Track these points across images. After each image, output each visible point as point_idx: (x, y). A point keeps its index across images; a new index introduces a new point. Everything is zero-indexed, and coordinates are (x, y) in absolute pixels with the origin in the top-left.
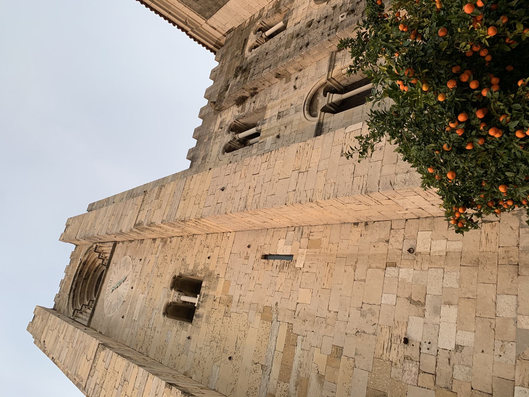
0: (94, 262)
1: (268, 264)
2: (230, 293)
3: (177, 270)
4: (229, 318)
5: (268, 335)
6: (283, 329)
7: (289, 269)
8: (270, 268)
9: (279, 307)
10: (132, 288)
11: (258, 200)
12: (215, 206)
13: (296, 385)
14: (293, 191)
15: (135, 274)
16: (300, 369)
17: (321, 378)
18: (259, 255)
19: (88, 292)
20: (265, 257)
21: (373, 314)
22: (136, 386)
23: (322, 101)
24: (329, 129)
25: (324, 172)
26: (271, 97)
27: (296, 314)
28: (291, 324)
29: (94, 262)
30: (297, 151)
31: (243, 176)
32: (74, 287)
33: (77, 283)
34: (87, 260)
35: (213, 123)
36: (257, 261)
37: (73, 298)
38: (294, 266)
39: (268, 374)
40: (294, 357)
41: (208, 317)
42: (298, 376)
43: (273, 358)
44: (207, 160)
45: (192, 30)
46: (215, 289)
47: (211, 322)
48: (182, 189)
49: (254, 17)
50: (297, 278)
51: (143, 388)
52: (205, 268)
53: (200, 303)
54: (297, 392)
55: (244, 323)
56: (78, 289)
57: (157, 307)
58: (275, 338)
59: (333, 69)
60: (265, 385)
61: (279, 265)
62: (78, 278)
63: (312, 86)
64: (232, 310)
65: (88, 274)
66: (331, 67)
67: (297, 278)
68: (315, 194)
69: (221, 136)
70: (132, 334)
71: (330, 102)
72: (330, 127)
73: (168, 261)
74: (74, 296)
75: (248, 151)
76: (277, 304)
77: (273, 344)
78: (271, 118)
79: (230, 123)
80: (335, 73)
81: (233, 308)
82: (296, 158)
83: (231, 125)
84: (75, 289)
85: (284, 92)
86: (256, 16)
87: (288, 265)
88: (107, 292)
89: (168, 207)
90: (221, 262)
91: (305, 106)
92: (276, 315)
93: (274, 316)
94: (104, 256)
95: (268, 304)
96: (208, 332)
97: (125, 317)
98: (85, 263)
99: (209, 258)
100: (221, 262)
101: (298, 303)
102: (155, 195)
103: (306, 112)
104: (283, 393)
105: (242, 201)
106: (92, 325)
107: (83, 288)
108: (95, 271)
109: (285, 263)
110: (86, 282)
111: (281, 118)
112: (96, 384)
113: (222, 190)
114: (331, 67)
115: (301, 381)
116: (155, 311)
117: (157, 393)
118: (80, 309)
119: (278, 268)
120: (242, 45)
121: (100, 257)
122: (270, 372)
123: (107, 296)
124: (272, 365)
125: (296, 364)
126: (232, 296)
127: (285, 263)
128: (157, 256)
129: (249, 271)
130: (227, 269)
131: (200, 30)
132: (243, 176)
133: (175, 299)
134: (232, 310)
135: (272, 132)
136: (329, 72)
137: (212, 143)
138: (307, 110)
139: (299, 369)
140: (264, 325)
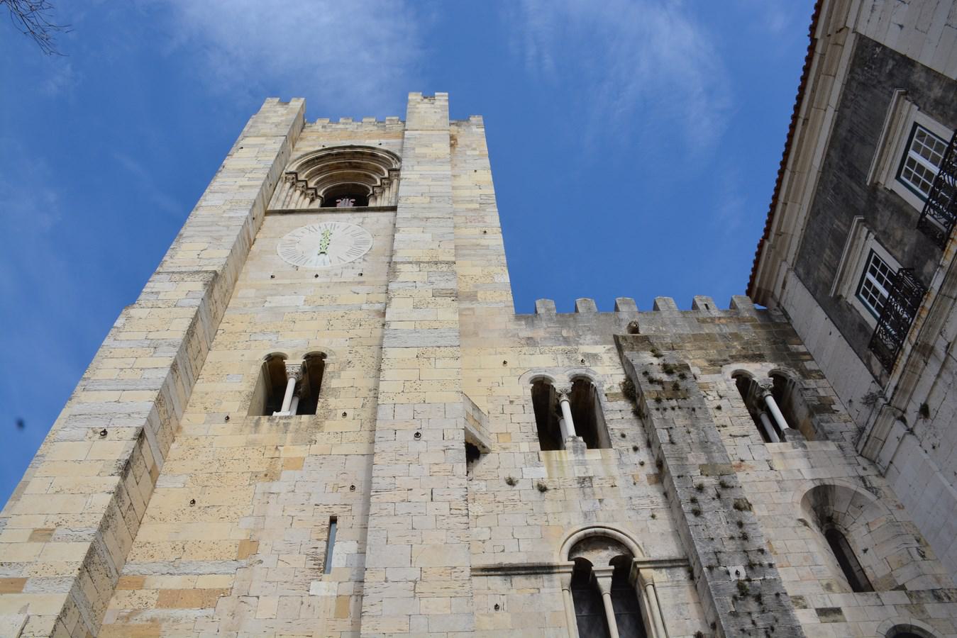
0: (379, 171)
1: (322, 531)
2: (286, 475)
3: (334, 357)
4: (248, 483)
5: (219, 559)
6: (221, 582)
7: (310, 571)
8: (314, 536)
9: (256, 566)
10: (317, 276)
11: (384, 512)
12: (392, 426)
13: (153, 620)
14: (386, 578)
15: (339, 272)
16: (171, 621)
18: (336, 511)
19: (331, 176)
20: (333, 520)
22: (147, 371)
23: (600, 560)
24: (538, 589)
25: (406, 628)
26: (625, 452)
27: (244, 599)
28: (231, 592)
29: (379, 171)
30: (455, 568)
31: (435, 468)
32: (335, 151)
33: (342, 154)
34: (377, 156)
35: (597, 338)
36: (328, 510)
37: (317, 158)
38: (313, 579)
39: (170, 571)
40: (187, 607)
41: (251, 444)
42: (163, 620)
43: (187, 574)
44: (525, 349)
45: (772, 247)
46: (295, 442)
47: (247, 452)
48: (439, 345)
49: (807, 360)
50: (296, 587)
51: (140, 387)
52: (331, 411)
53: (277, 421)
54: (144, 623)
55: (240, 514)
56: (333, 159)
57: (281, 339)
58: (214, 570)
59: (655, 568)
60: (156, 569)
61: (319, 551)
62: (349, 153)
63: (632, 536)
64: (259, 485)
65: (357, 166)
66: (658, 564)
67: (296, 587)
68: (372, 619)
69: (569, 364)
70: (245, 305)
71: (597, 575)
72: (541, 590)
73: (352, 333)
74: (321, 157)
75: (529, 434)
76: (261, 562)
77: (207, 570)
78: (583, 463)
79: (591, 375)
80: (646, 573)
81: (262, 486)
83: (588, 378)
84: (332, 155)
85: (630, 477)
86: (809, 365)
87: (317, 567)
88: (316, 226)
89: (411, 326)
91: (593, 530)
92: (244, 565)
93: (244, 562)
94: (385, 186)
95: (262, 546)
96: (232, 450)
97: (273, 281)
98: (373, 156)
99: (345, 414)
101: (258, 597)
102: (442, 285)
103: (582, 533)
104: (145, 600)
105: (388, 480)
106: (269, 218)
107: (338, 167)
108: (366, 175)
109: (320, 562)
110: (346, 167)
111: (579, 485)
112: (158, 293)
113: (417, 434)
114: (658, 564)
115: (157, 627)
116: (273, 337)
117: (132, 415)
118: (299, 179)
119: (314, 550)
120: (750, 352)
121: (383, 181)
122: (171, 574)
123: (311, 229)
124: (179, 574)
125: (178, 612)
126: (278, 480)
127: (320, 562)
128: (364, 306)
129: (313, 501)
130: (321, 457)
131: (775, 261)
132: (435, 468)
133: (288, 370)
134: (259, 485)
135: (556, 474)
136: (649, 562)
137: (557, 347)
138: (585, 535)
139: (172, 619)
140: (233, 547)
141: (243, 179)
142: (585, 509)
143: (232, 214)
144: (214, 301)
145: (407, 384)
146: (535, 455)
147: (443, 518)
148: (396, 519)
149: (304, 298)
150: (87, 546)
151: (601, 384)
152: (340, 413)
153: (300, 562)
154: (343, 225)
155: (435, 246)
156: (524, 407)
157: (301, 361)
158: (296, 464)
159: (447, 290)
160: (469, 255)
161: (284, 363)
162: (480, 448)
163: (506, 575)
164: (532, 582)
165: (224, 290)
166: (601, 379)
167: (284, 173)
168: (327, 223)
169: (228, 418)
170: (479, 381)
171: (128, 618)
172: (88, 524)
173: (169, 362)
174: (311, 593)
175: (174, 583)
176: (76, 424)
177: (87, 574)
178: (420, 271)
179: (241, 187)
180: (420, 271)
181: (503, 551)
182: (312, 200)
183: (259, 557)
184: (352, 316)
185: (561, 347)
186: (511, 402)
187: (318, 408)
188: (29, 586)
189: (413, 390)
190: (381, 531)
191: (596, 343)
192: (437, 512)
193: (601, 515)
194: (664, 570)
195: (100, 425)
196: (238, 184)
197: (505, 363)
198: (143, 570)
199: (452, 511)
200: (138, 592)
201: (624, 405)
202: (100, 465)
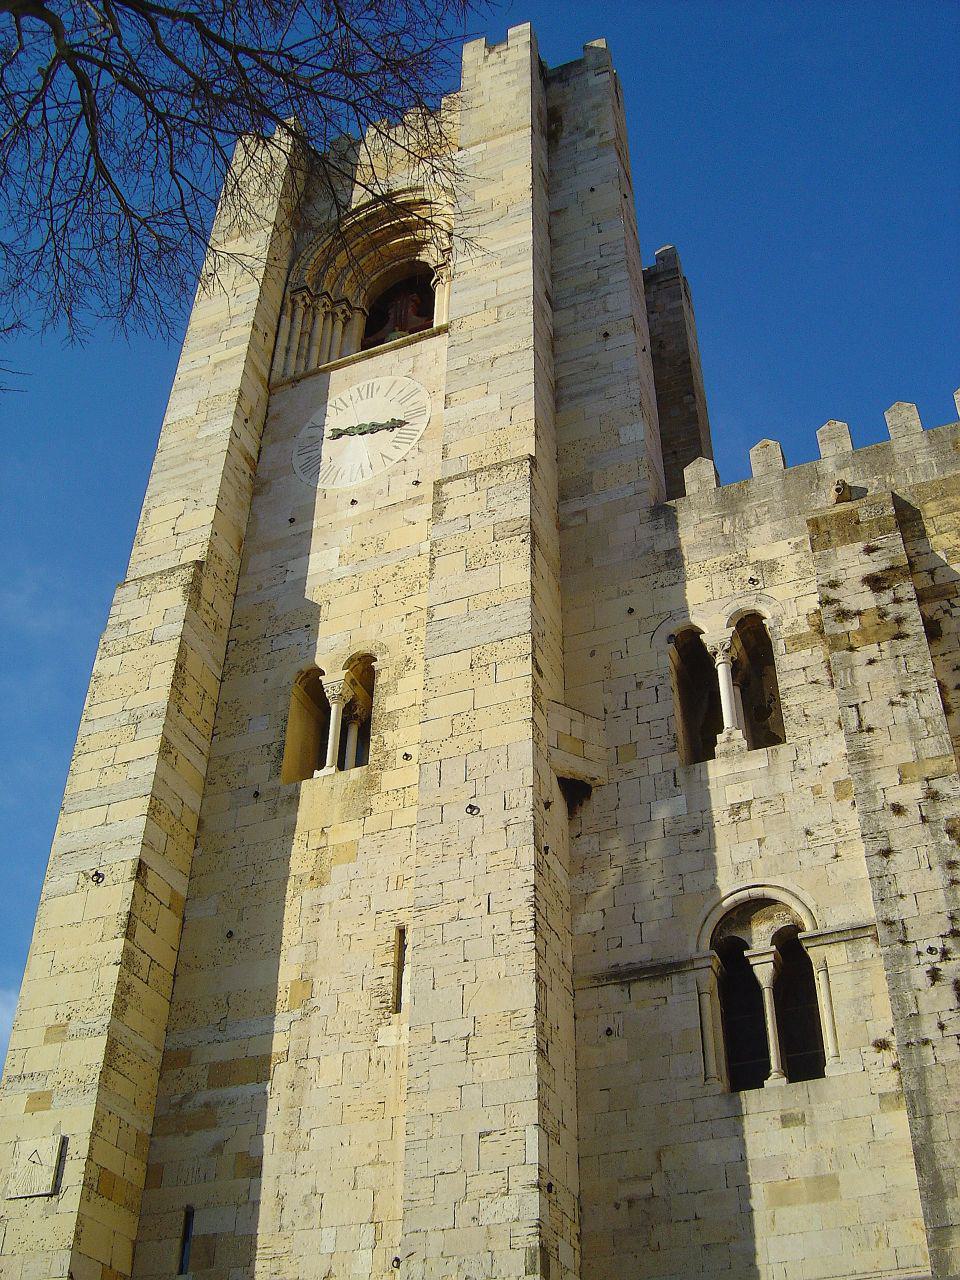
8: (380, 961)
11: (429, 942)
13: (207, 1105)
17: (218, 1148)
21: (308, 1217)
31: (493, 860)
67: (359, 1038)
68: (419, 1097)
71: (752, 961)
82: (502, 1014)
90: (394, 805)
100: (394, 805)
123: (342, 406)
125: (231, 1091)
129: (374, 908)
132: (493, 860)
134: (305, 894)
141: (217, 346)
142: (737, 859)
143: (209, 432)
144: (208, 607)
145: (458, 720)
146: (670, 777)
147: (502, 937)
148: (446, 949)
149: (337, 551)
150: (103, 1040)
151: (778, 621)
152: (400, 753)
153: (361, 1003)
154: (384, 382)
155: (503, 421)
156: (657, 690)
157: (342, 674)
158: (351, 851)
159: (513, 520)
160: (580, 395)
161: (321, 681)
162: (588, 781)
163: (622, 983)
164: (659, 987)
165: (222, 575)
166: (778, 611)
167: (288, 293)
168: (360, 385)
169: (257, 794)
170: (593, 654)
171: (180, 1105)
172: (100, 1012)
173: (154, 745)
174: (379, 1044)
175: (222, 1052)
176: (63, 869)
177: (113, 1073)
178: (477, 490)
179: (216, 366)
180: (477, 490)
181: (620, 945)
182: (347, 320)
183: (315, 1002)
184: (408, 572)
185: (718, 559)
186: (639, 685)
187: (371, 753)
188: (57, 1101)
189: (464, 730)
190: (426, 971)
191: (777, 537)
192: (494, 932)
193: (759, 864)
194: (843, 944)
195: (90, 864)
196: (213, 360)
197: (631, 611)
198: (188, 1041)
199: (516, 926)
200: (185, 1070)
201: (813, 656)
202: (100, 927)
